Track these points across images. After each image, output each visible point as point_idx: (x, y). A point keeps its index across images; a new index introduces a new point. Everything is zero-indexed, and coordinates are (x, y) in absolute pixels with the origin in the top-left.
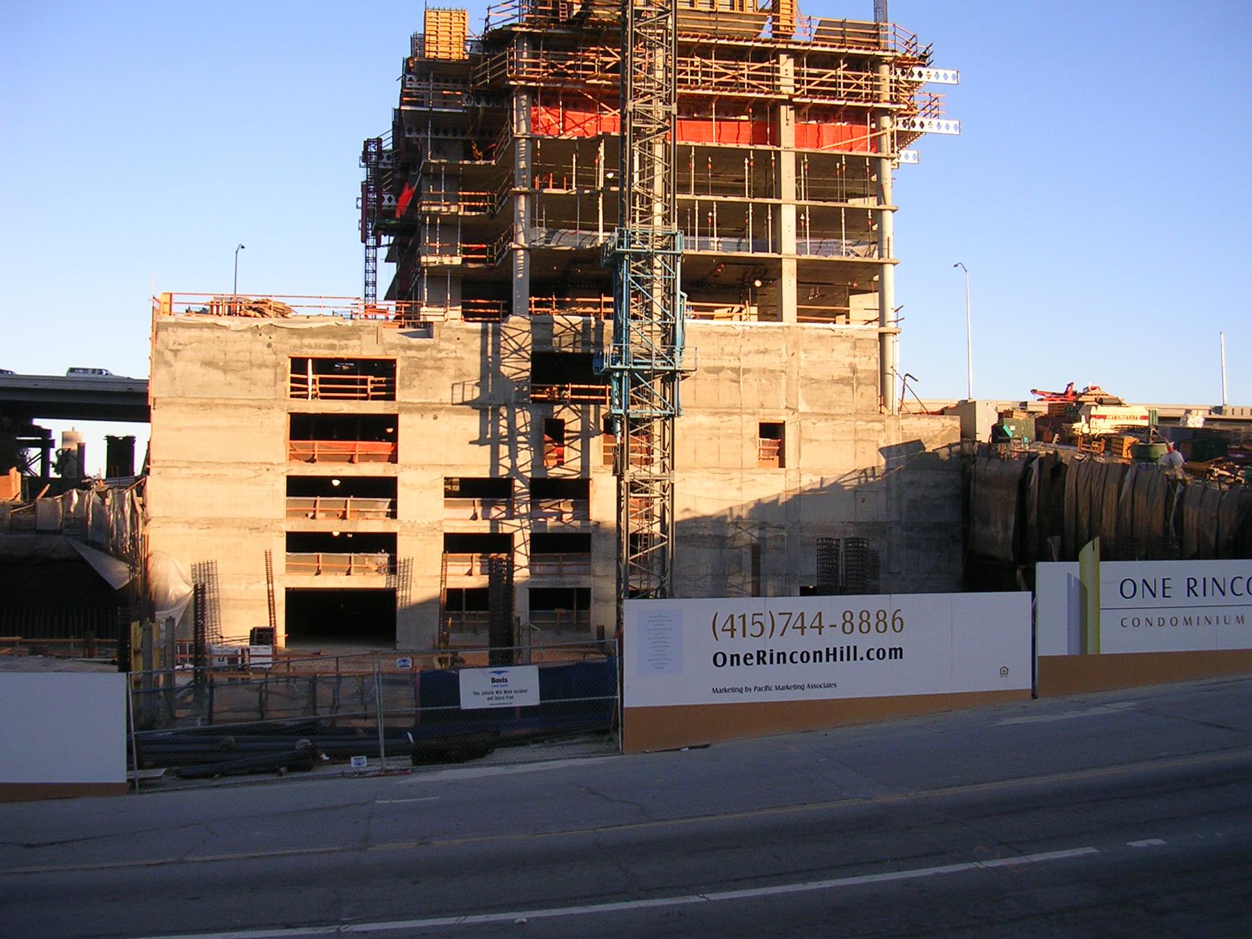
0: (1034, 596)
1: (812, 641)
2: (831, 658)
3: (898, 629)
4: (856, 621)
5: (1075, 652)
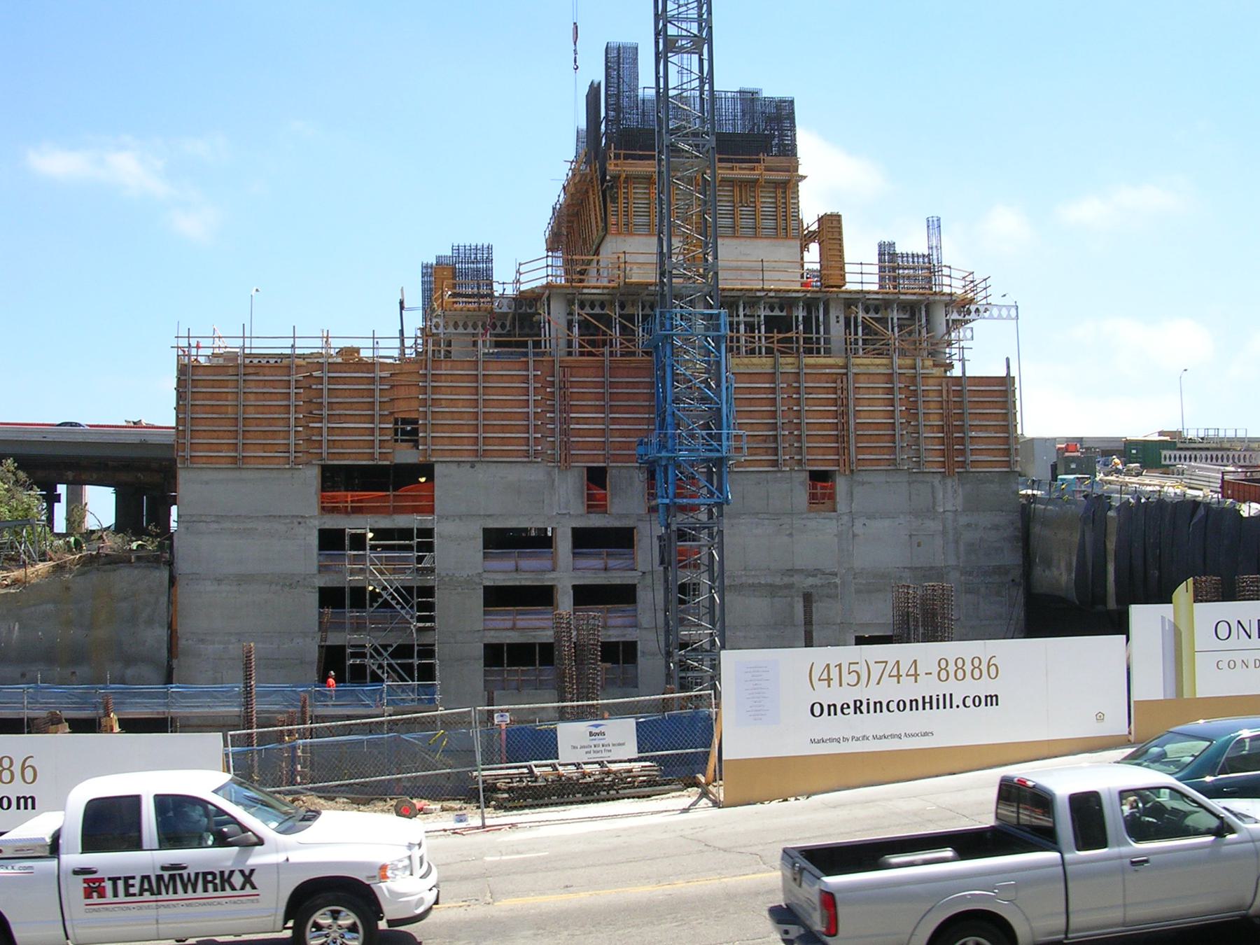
0: (1128, 640)
1: (909, 690)
2: (927, 706)
3: (993, 675)
4: (952, 668)
5: (1171, 695)
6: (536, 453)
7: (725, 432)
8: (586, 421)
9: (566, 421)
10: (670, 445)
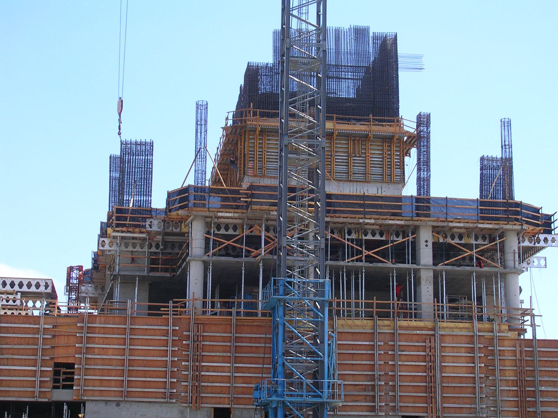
6: (172, 396)
7: (326, 380)
8: (215, 369)
9: (198, 369)
10: (279, 389)
